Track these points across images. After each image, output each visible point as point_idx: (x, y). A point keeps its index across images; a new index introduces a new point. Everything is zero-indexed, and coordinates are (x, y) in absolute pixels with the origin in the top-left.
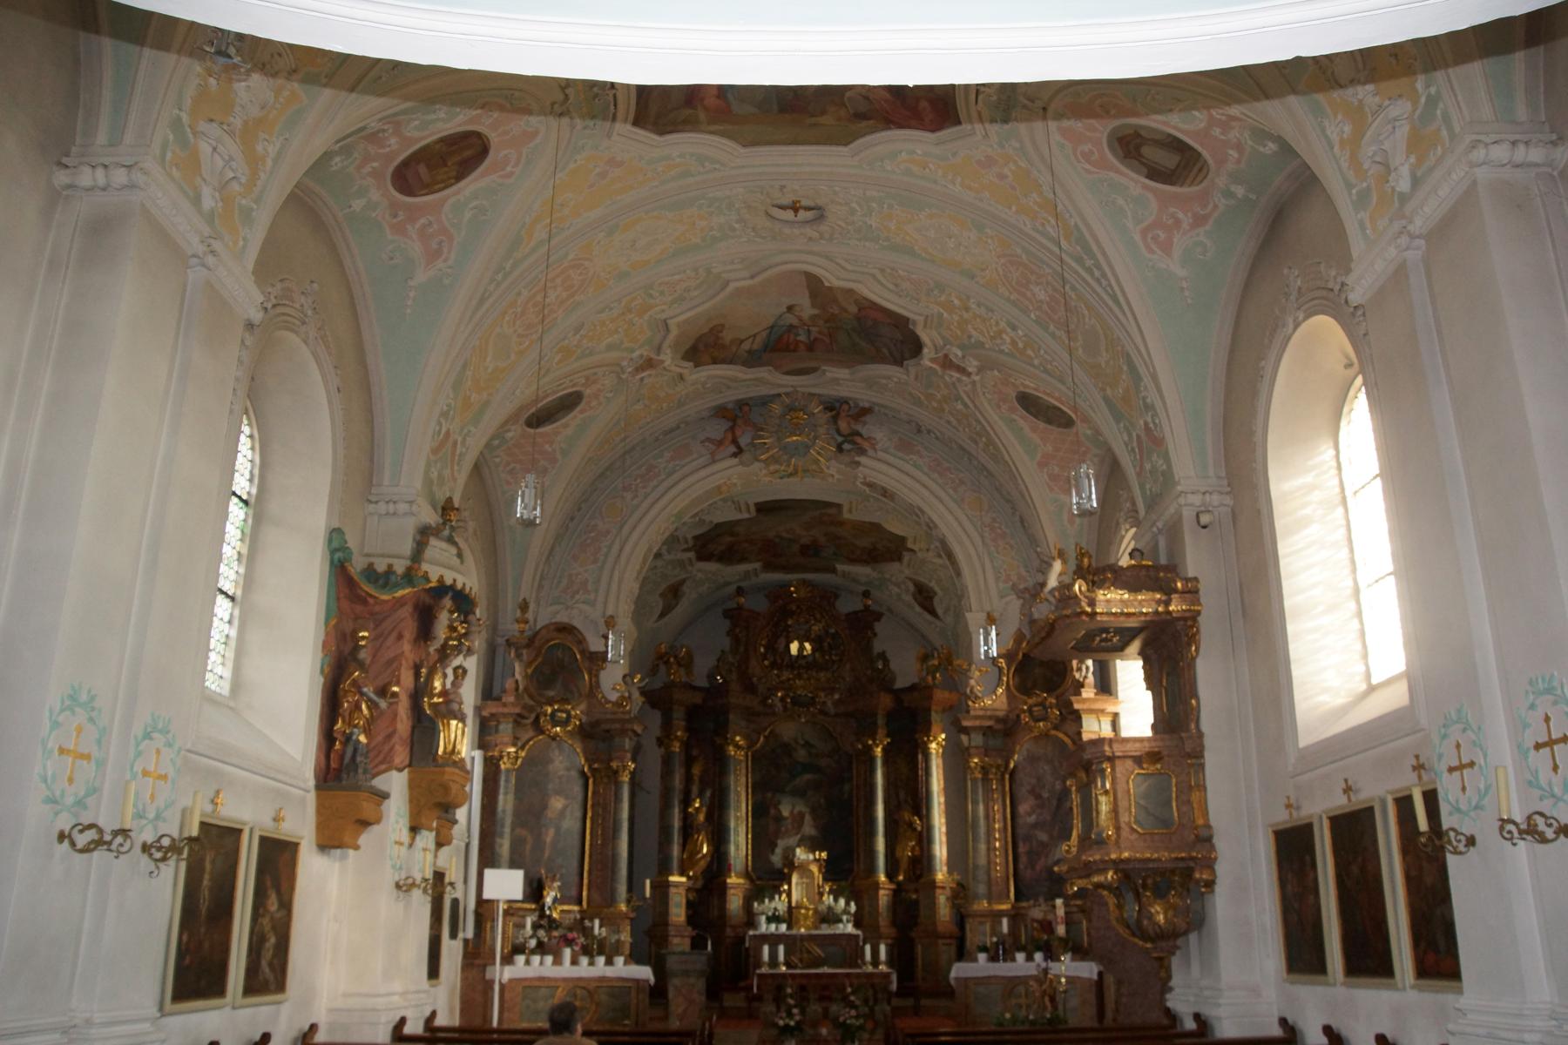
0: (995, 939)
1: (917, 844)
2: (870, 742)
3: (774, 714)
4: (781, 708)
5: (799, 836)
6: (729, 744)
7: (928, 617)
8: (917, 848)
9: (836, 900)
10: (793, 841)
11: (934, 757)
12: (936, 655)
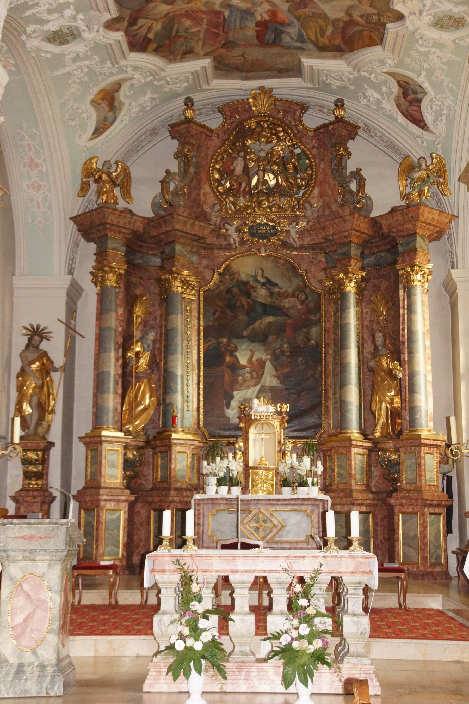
1: (396, 395)
2: (342, 276)
3: (229, 247)
4: (237, 239)
5: (258, 387)
6: (176, 278)
8: (397, 400)
9: (300, 460)
10: (252, 391)
12: (424, 166)
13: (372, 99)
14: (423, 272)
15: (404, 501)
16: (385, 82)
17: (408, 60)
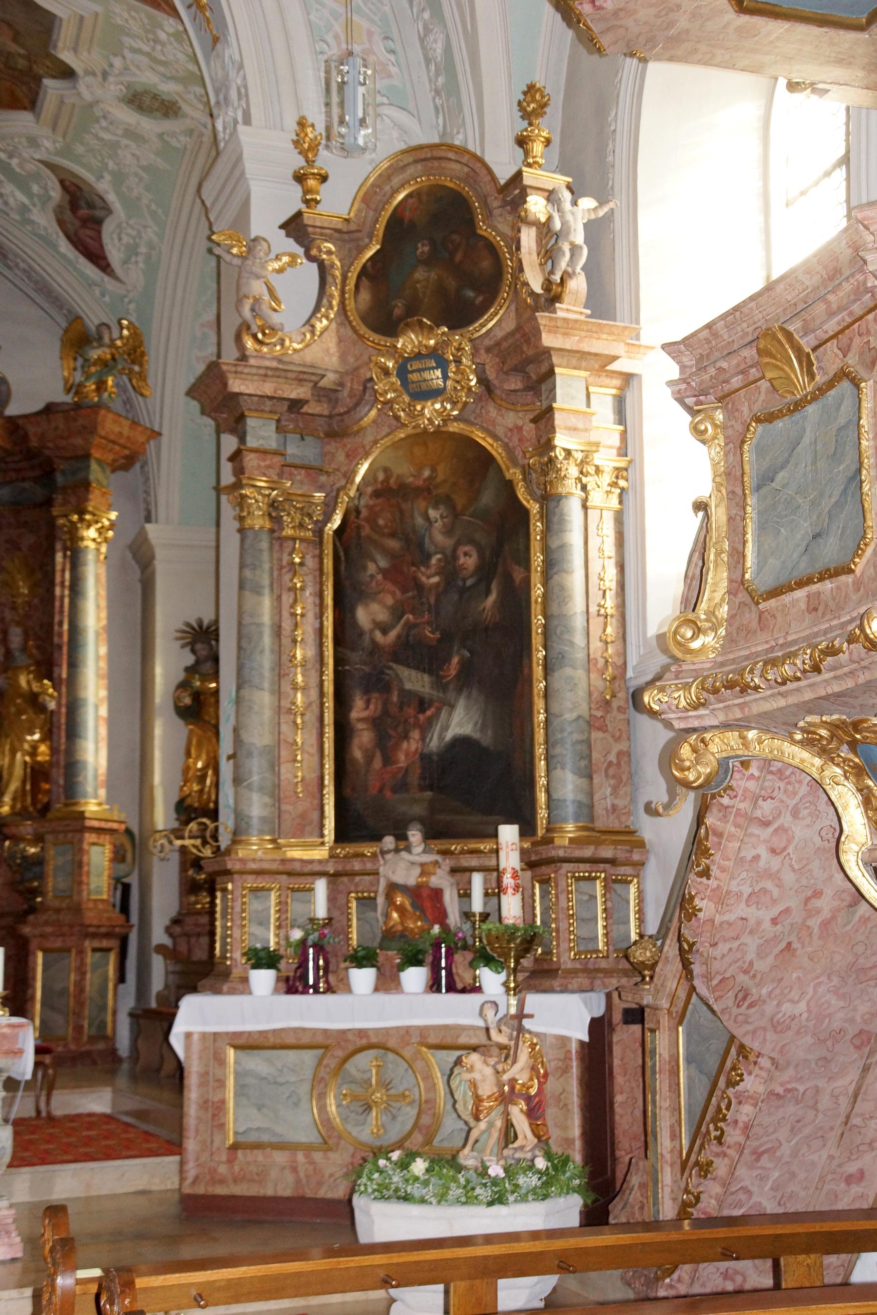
0: (297, 935)
1: (42, 740)
7: (90, 270)
11: (91, 557)
12: (106, 340)
13: (11, 201)
14: (99, 525)
15: (49, 929)
16: (36, 177)
17: (80, 149)
